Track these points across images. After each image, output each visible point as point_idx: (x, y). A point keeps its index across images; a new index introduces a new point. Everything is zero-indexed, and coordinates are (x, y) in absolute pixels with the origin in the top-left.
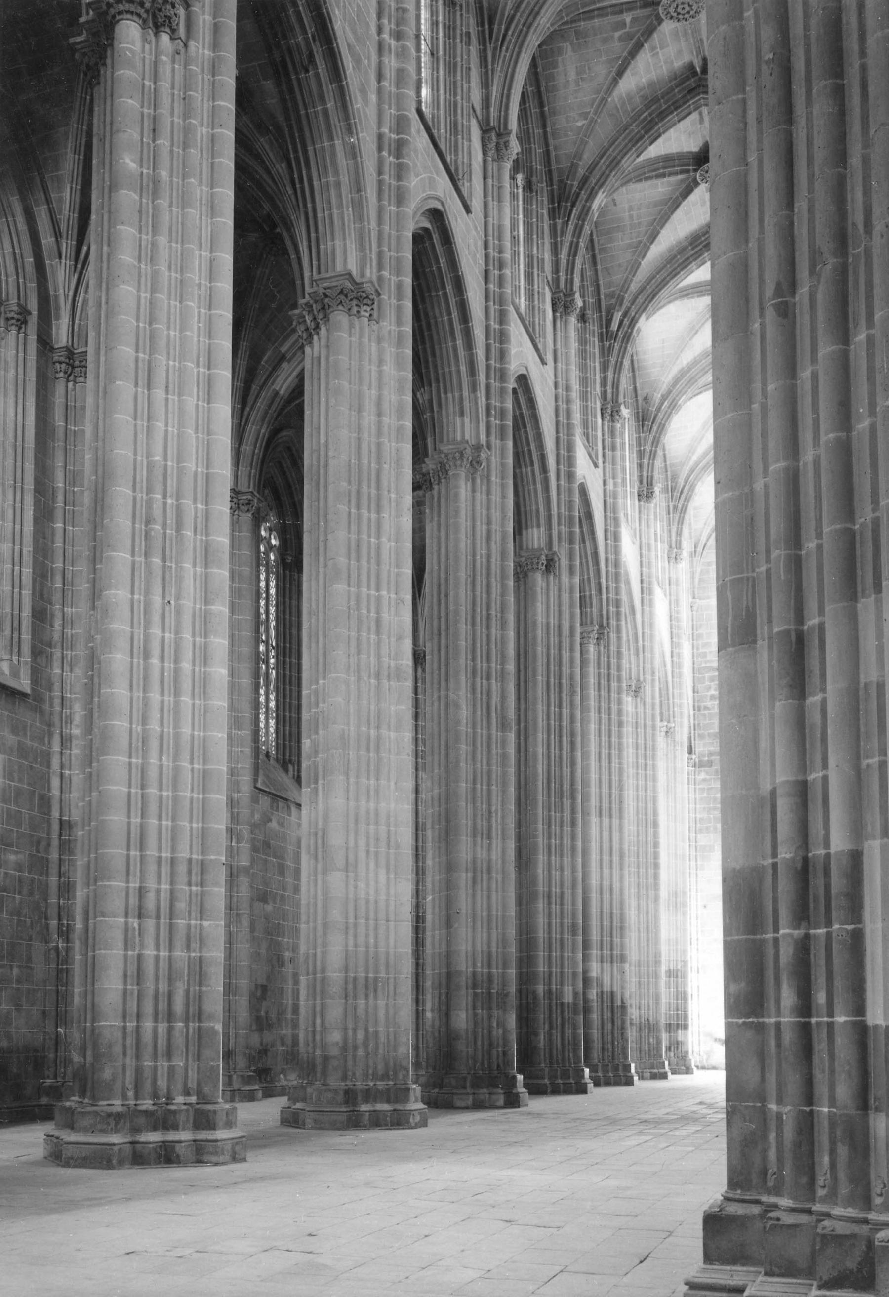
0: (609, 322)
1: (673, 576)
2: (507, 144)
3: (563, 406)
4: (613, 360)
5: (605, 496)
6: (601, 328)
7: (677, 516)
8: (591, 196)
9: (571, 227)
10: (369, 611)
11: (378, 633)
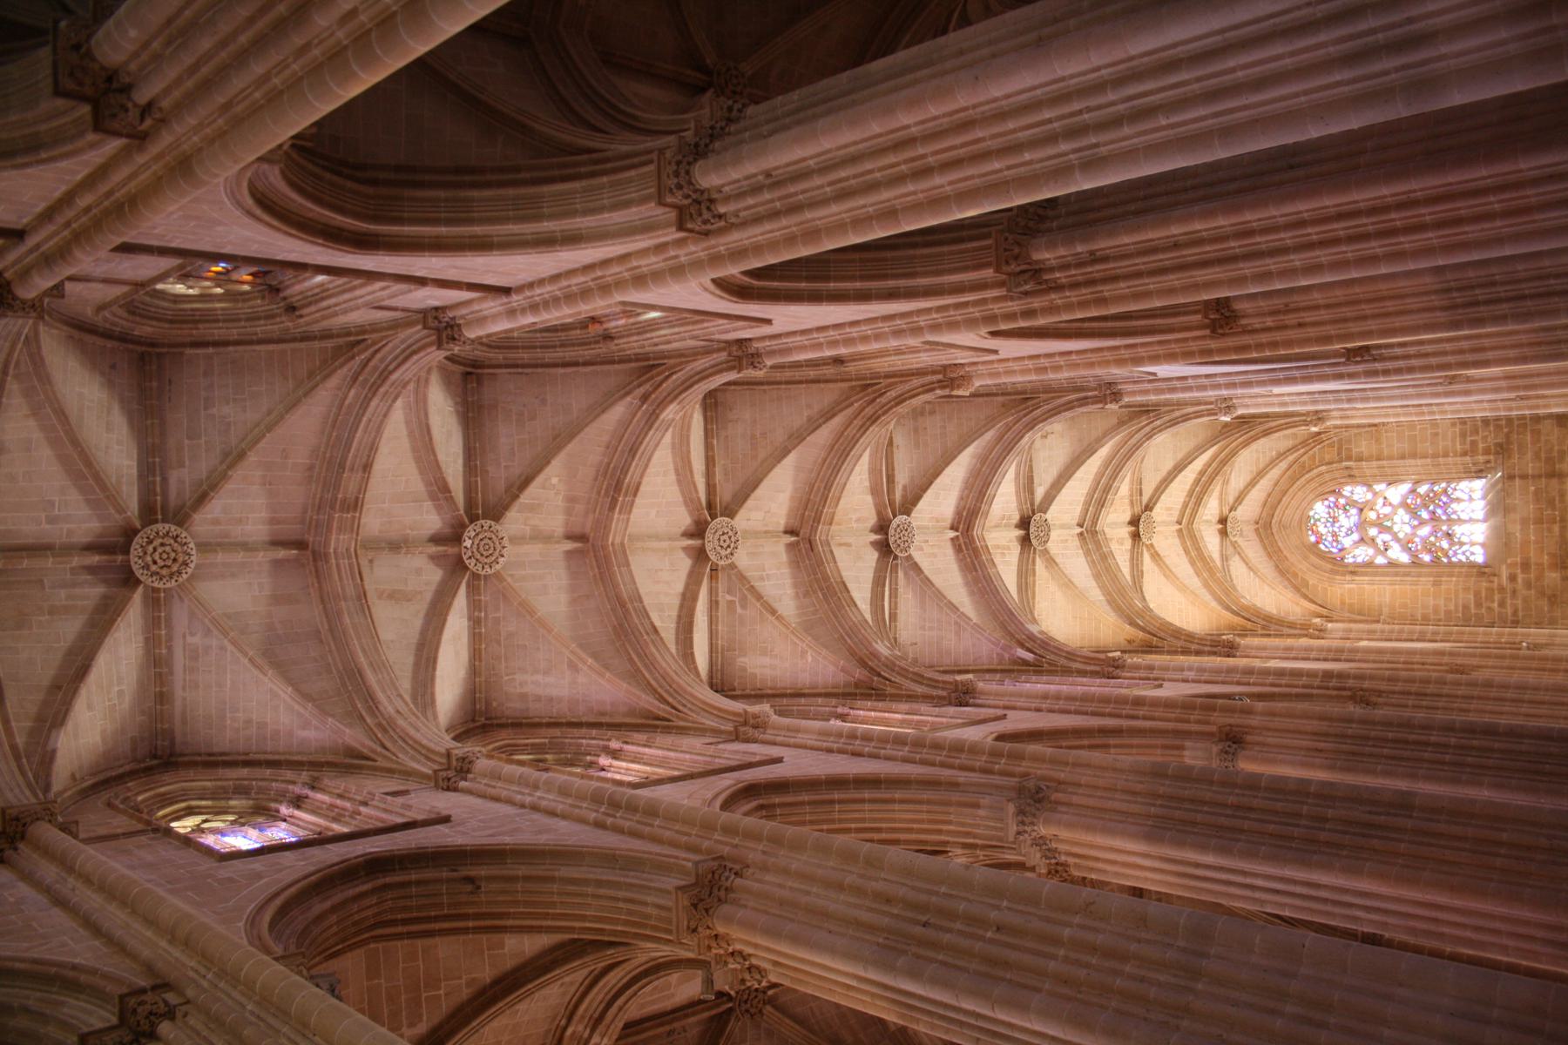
0: (1025, 662)
1: (1340, 634)
2: (755, 716)
3: (1061, 704)
4: (1063, 661)
7: (1273, 627)
8: (875, 655)
9: (898, 679)
10: (1088, 966)
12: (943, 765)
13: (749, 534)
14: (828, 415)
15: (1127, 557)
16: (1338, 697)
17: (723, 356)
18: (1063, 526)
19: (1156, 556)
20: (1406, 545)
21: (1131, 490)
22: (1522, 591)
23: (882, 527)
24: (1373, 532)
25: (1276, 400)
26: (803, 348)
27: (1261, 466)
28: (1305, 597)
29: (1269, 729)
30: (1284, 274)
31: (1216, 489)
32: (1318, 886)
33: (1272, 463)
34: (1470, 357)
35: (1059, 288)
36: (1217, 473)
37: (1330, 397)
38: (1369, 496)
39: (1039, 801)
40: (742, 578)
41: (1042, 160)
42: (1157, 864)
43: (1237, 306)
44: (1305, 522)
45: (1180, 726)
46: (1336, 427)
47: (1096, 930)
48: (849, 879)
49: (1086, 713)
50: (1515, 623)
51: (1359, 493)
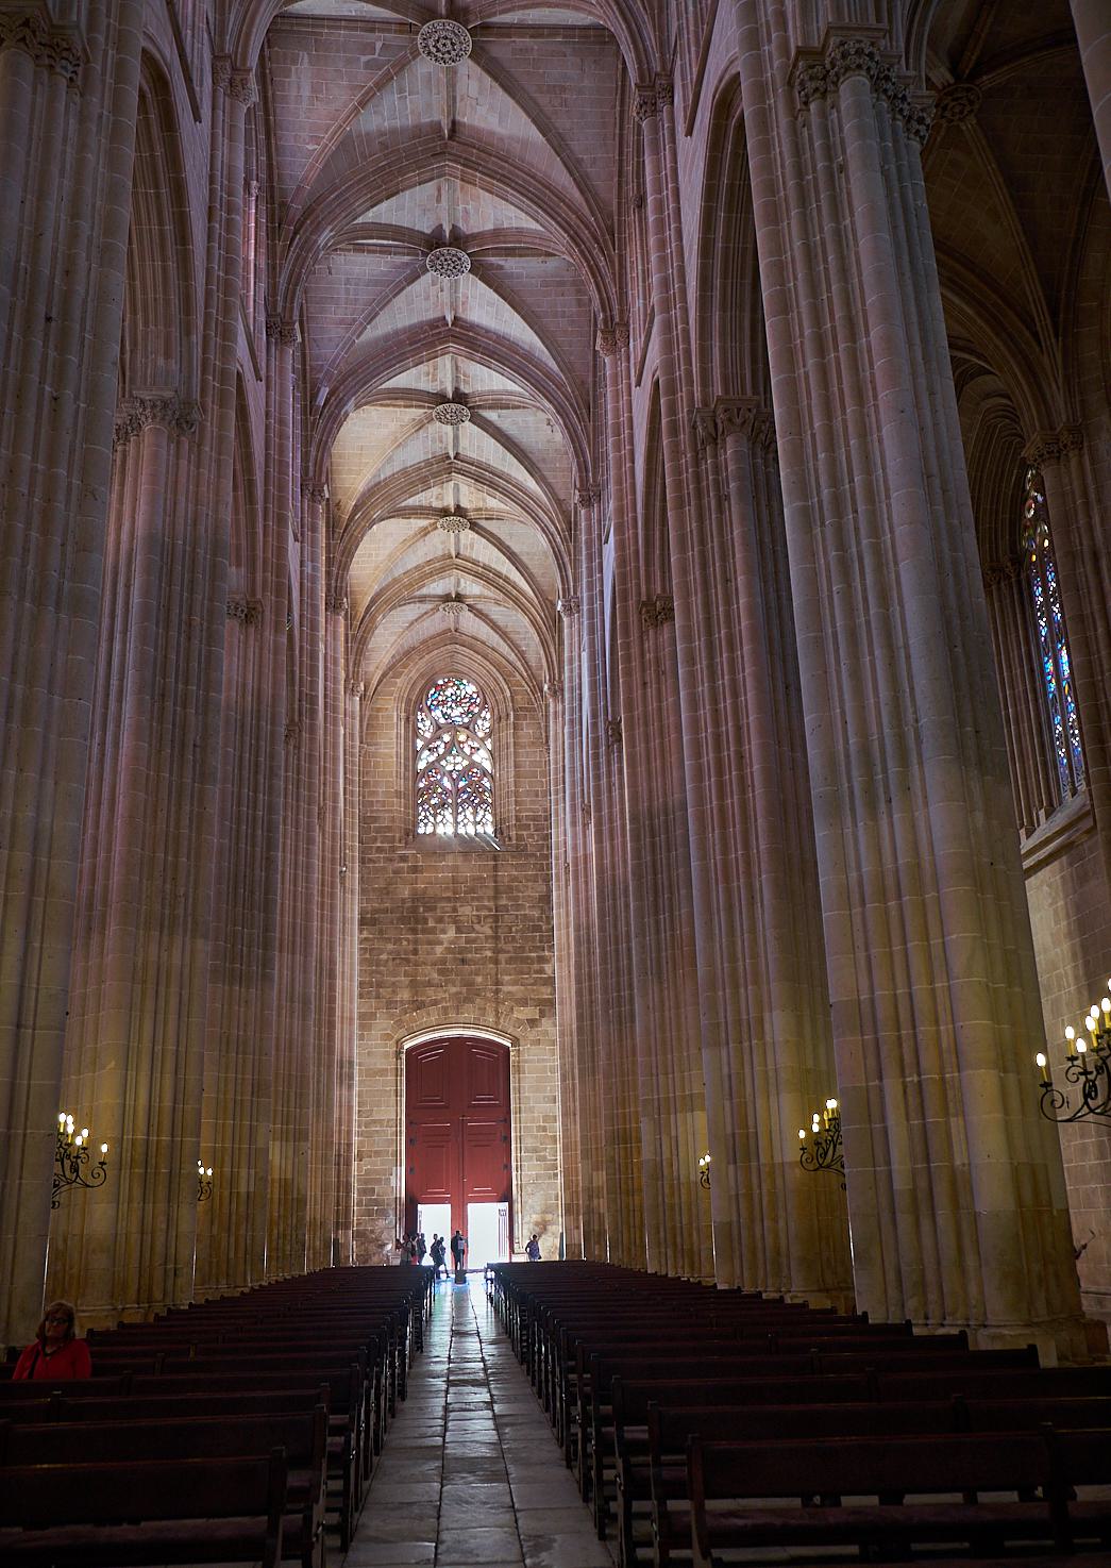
0: (314, 396)
1: (349, 708)
2: (244, 82)
4: (317, 437)
5: (301, 578)
6: (305, 400)
8: (318, 229)
9: (292, 255)
10: (31, 493)
11: (45, 531)
12: (207, 315)
13: (452, 74)
14: (583, 184)
15: (425, 503)
16: (293, 709)
17: (657, 67)
18: (456, 438)
19: (425, 532)
20: (431, 766)
21: (492, 510)
22: (390, 867)
23: (458, 240)
24: (447, 738)
25: (575, 654)
26: (657, 170)
27: (511, 636)
28: (384, 675)
29: (261, 649)
30: (692, 676)
31: (491, 593)
32: (120, 700)
33: (514, 646)
34: (606, 828)
35: (697, 462)
36: (507, 594)
37: (576, 704)
38: (481, 734)
39: (178, 425)
40: (401, 66)
41: (816, 470)
42: (124, 547)
43: (666, 627)
44: (458, 676)
45: (259, 563)
46: (547, 706)
47: (68, 502)
48: (85, 226)
49: (267, 466)
50: (362, 861)
51: (483, 726)
